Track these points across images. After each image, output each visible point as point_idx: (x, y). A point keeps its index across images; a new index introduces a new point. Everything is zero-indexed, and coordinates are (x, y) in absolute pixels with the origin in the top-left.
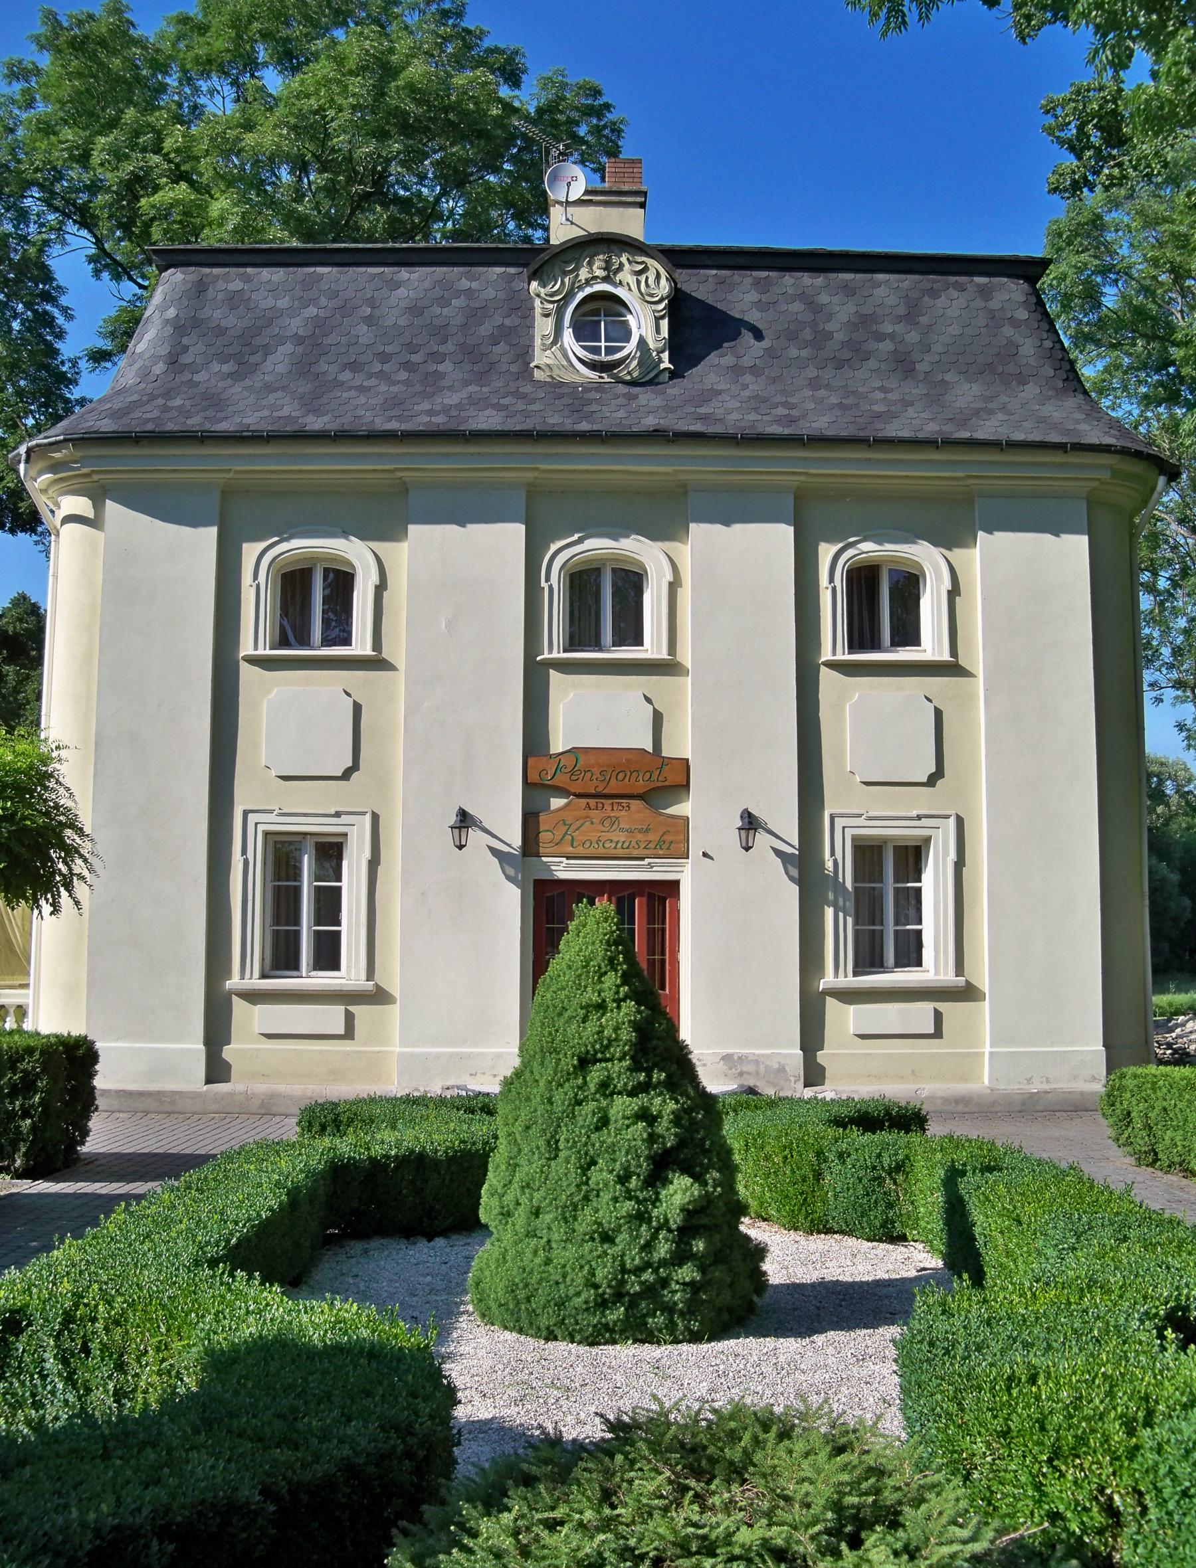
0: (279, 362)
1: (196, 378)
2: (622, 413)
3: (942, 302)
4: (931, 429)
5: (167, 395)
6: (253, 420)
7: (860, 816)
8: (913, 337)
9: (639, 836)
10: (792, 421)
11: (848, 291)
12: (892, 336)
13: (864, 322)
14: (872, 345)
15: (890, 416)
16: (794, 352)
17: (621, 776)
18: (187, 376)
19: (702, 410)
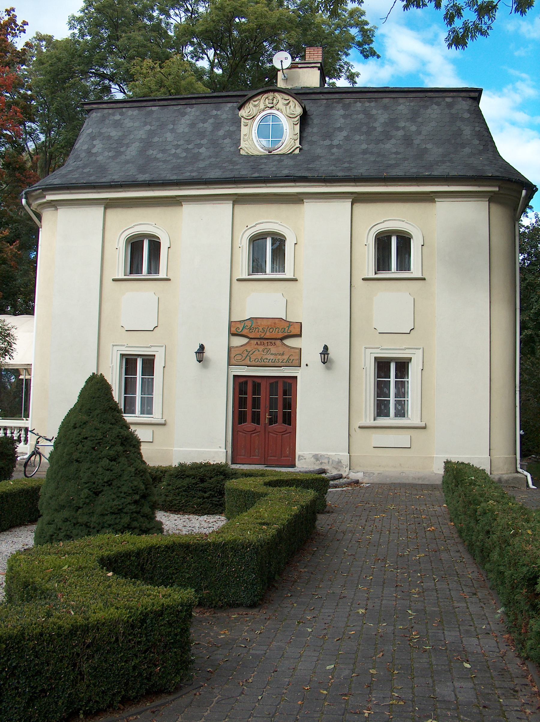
1: (98, 159)
2: (274, 169)
3: (429, 111)
5: (85, 166)
6: (116, 177)
7: (378, 348)
8: (414, 128)
9: (279, 357)
10: (350, 169)
11: (386, 108)
12: (404, 128)
13: (392, 123)
14: (394, 133)
15: (396, 165)
16: (357, 137)
17: (271, 330)
18: (93, 158)
19: (311, 166)
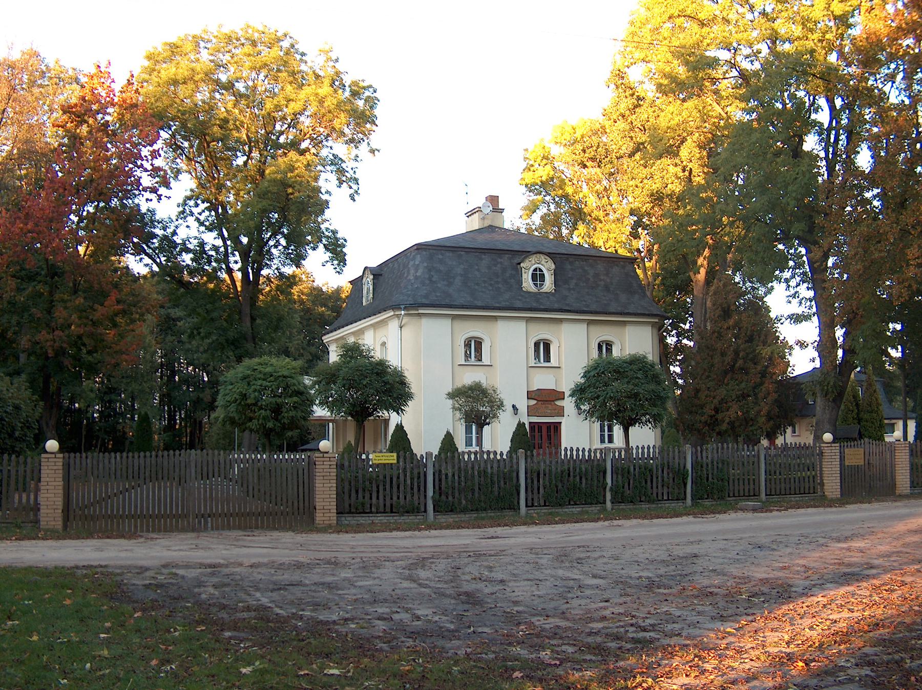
0: (458, 281)
4: (619, 309)
10: (588, 306)
